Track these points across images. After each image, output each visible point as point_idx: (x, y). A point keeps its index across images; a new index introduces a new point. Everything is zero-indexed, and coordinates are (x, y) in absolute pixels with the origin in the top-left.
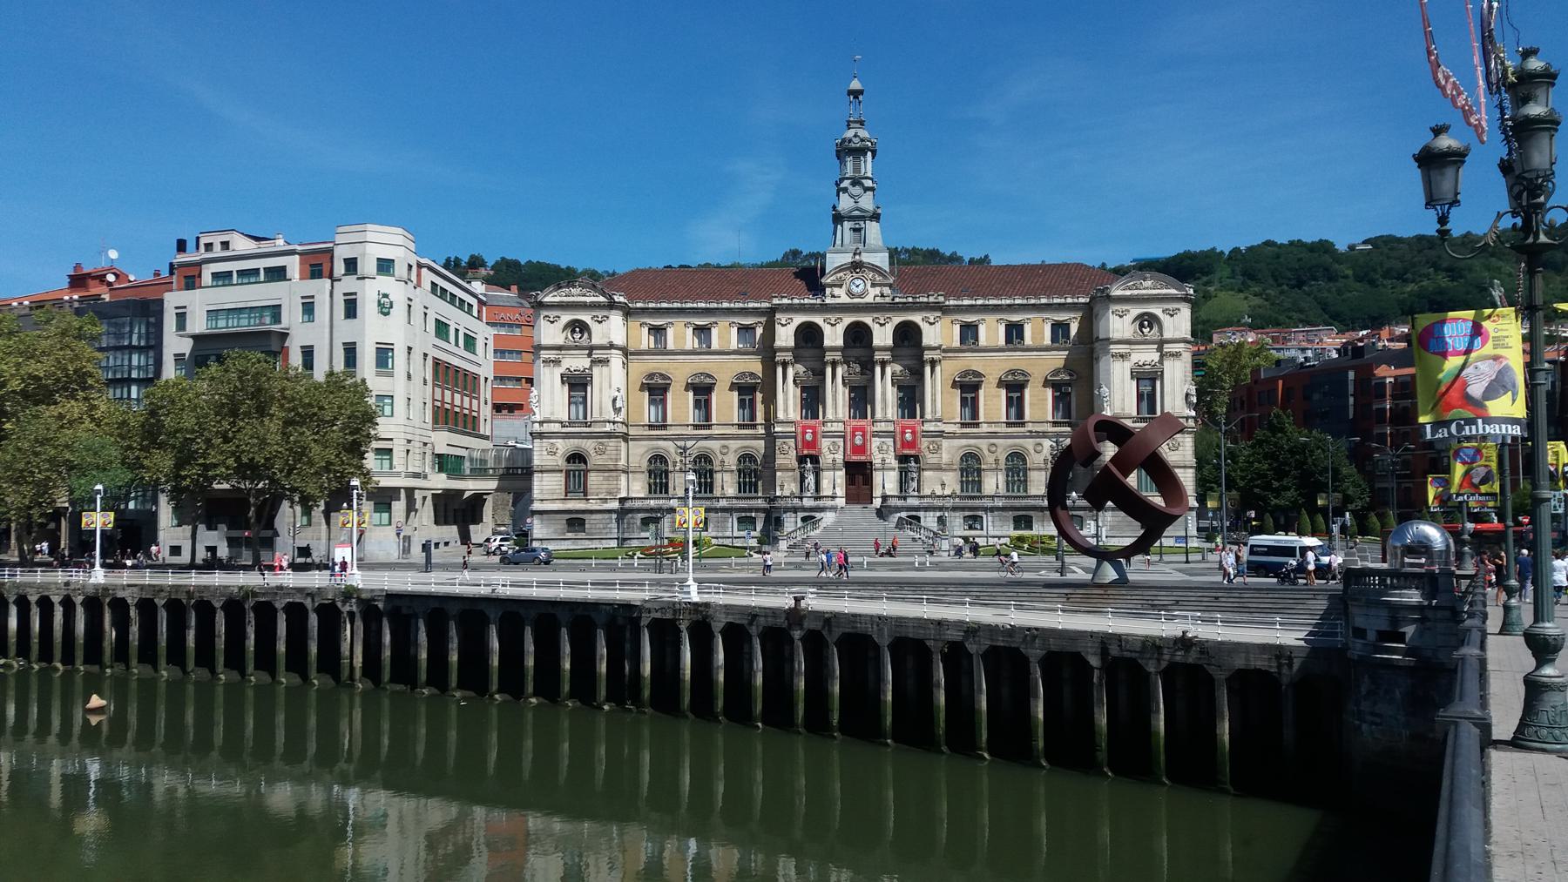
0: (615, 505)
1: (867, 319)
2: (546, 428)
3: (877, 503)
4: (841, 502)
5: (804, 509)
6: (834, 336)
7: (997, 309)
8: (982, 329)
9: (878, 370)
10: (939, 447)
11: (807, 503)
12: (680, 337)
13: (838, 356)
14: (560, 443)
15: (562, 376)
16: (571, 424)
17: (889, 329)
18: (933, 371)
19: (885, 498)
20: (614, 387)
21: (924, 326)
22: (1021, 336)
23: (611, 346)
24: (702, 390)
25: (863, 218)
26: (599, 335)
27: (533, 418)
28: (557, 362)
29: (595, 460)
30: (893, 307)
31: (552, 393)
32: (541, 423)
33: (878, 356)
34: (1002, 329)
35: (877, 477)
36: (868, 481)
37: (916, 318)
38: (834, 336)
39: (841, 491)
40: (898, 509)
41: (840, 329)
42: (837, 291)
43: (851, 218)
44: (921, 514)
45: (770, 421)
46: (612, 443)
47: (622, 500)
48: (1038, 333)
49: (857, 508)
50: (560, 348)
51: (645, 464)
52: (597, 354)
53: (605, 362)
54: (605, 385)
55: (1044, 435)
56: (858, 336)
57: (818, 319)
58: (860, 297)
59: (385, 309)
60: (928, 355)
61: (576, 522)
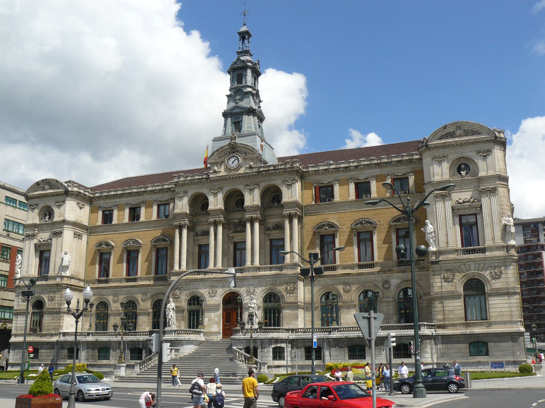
1: (241, 187)
8: (337, 189)
9: (248, 226)
22: (368, 191)
23: (64, 222)
29: (48, 304)
34: (352, 187)
41: (220, 196)
56: (235, 200)
57: (205, 191)
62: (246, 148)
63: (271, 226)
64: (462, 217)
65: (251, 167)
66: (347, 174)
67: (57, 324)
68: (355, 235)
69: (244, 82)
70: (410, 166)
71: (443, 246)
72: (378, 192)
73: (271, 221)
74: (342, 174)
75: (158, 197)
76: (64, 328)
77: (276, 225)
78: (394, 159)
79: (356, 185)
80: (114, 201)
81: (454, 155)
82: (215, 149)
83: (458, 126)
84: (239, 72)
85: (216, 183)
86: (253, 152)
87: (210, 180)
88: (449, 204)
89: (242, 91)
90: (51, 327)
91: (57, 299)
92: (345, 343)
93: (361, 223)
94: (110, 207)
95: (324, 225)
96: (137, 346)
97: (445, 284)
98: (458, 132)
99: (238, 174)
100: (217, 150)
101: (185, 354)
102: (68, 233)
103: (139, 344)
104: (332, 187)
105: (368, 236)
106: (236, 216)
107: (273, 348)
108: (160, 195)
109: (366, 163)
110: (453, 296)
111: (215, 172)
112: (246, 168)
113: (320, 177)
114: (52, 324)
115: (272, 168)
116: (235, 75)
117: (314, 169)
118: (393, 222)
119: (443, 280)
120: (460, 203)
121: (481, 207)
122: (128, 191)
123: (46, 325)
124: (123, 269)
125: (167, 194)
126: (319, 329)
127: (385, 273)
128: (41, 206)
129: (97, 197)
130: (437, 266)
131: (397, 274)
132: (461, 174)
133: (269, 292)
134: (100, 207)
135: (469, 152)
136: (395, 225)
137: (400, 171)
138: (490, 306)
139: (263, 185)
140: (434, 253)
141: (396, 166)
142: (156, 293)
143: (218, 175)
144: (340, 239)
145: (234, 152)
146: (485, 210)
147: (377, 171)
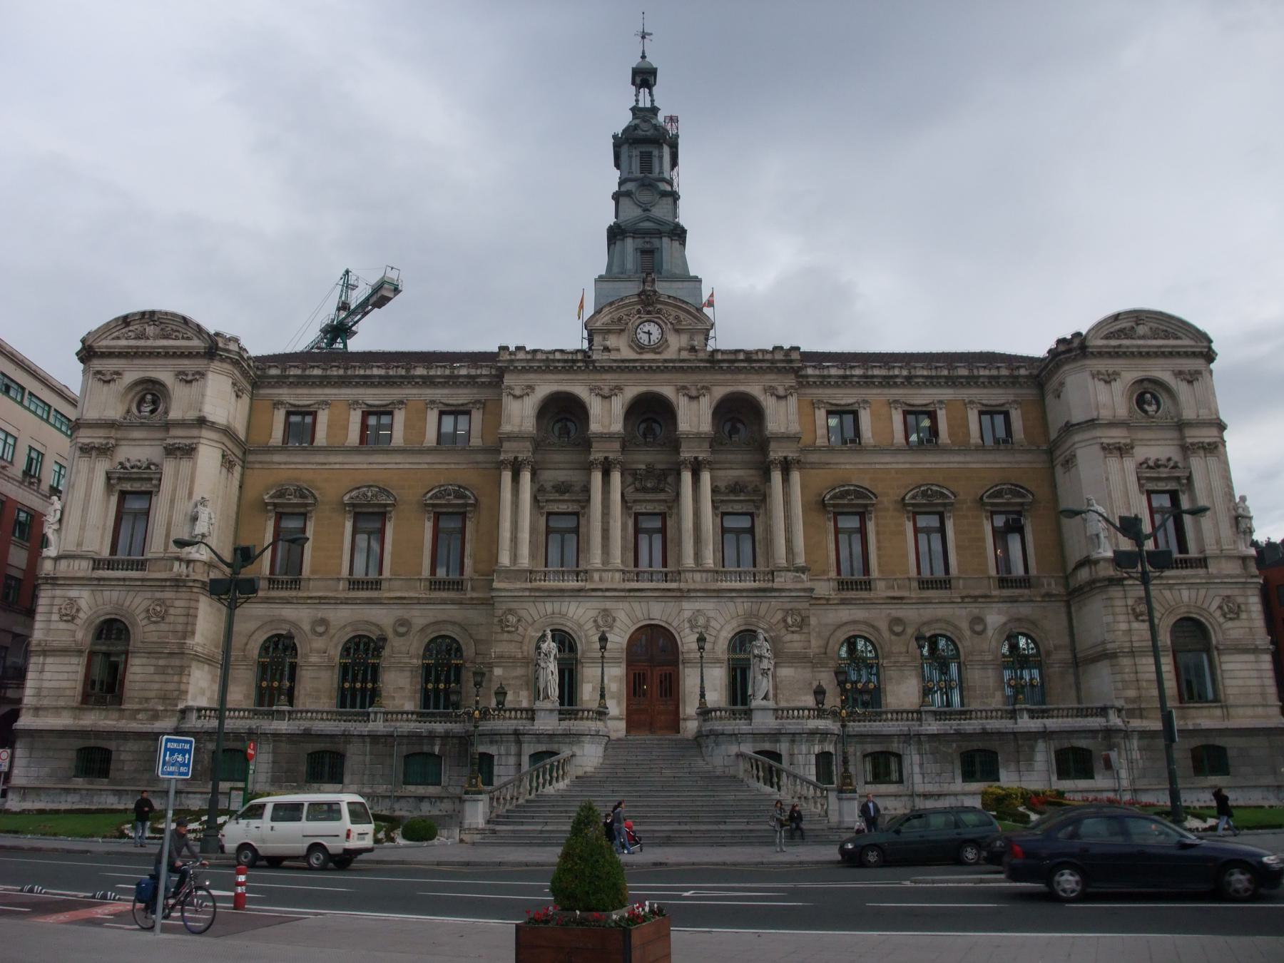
1: (668, 391)
3: (691, 727)
4: (617, 728)
5: (539, 736)
7: (888, 382)
8: (865, 417)
9: (687, 477)
10: (803, 623)
11: (547, 723)
12: (338, 426)
13: (614, 451)
14: (84, 597)
15: (109, 477)
16: (110, 565)
17: (705, 407)
18: (786, 480)
19: (705, 712)
20: (197, 497)
21: (769, 403)
25: (659, 234)
27: (46, 552)
29: (144, 632)
31: (85, 510)
32: (57, 559)
33: (686, 454)
34: (897, 417)
35: (689, 680)
36: (670, 687)
37: (754, 388)
38: (606, 416)
39: (615, 708)
40: (735, 737)
41: (618, 406)
42: (612, 341)
43: (637, 233)
44: (783, 747)
45: (490, 569)
46: (179, 602)
47: (184, 712)
48: (959, 426)
49: (644, 737)
51: (254, 649)
54: (182, 493)
56: (651, 415)
57: (581, 391)
58: (654, 350)
60: (776, 453)
62: (680, 308)
63: (722, 485)
64: (1153, 496)
65: (693, 349)
66: (886, 391)
67: (171, 687)
68: (908, 518)
69: (657, 170)
70: (1011, 391)
72: (950, 435)
73: (721, 473)
74: (875, 391)
75: (440, 394)
76: (189, 696)
77: (737, 483)
78: (982, 372)
79: (906, 413)
80: (318, 391)
82: (604, 301)
84: (645, 148)
85: (608, 376)
86: (695, 317)
87: (595, 367)
89: (656, 188)
90: (152, 694)
91: (171, 619)
92: (954, 745)
93: (924, 494)
94: (309, 406)
95: (848, 493)
96: (426, 749)
97: (1135, 625)
99: (666, 361)
100: (611, 304)
101: (588, 769)
102: (209, 456)
103: (433, 745)
104: (855, 414)
105: (934, 522)
106: (642, 459)
107: (817, 756)
108: (445, 391)
109: (925, 373)
111: (607, 349)
112: (680, 350)
113: (829, 391)
114: (156, 686)
115: (741, 356)
116: (636, 152)
117: (817, 372)
118: (989, 497)
119: (1132, 618)
120: (1149, 467)
121: (1189, 478)
122: (362, 372)
123: (137, 686)
124: (341, 557)
125: (460, 391)
126: (997, 711)
127: (975, 602)
129: (273, 377)
130: (1120, 588)
131: (1000, 605)
132: (1146, 412)
133: (743, 628)
134: (277, 404)
136: (993, 505)
137: (995, 396)
138: (1226, 675)
139: (719, 392)
141: (985, 387)
142: (433, 620)
143: (614, 356)
144: (877, 525)
145: (649, 313)
146: (1199, 483)
147: (946, 394)
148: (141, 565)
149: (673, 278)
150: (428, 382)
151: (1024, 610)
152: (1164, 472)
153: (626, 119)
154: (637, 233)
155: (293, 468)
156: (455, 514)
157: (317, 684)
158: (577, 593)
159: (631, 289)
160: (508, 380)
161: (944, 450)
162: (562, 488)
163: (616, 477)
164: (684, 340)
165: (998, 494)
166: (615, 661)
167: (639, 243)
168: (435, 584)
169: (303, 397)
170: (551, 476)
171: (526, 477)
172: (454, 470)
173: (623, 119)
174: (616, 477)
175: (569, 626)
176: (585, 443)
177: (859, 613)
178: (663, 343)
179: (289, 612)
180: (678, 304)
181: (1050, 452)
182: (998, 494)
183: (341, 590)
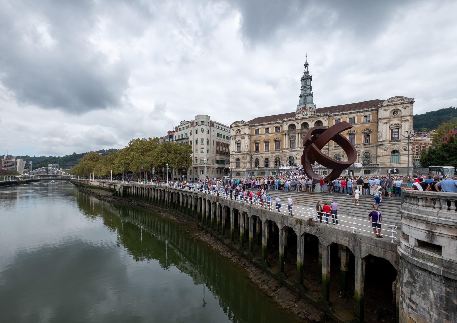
0: (245, 170)
1: (307, 122)
2: (232, 153)
6: (298, 126)
7: (346, 114)
12: (262, 131)
13: (299, 131)
21: (323, 121)
23: (245, 134)
24: (267, 143)
25: (307, 96)
26: (243, 132)
28: (235, 139)
30: (314, 117)
37: (321, 119)
38: (298, 126)
41: (300, 125)
42: (299, 115)
43: (303, 96)
46: (245, 156)
48: (359, 120)
50: (235, 136)
52: (243, 136)
53: (244, 138)
55: (361, 147)
57: (294, 123)
59: (202, 131)
61: (238, 173)
71: (384, 139)
81: (392, 108)
83: (395, 98)
88: (388, 125)
98: (395, 100)
110: (387, 155)
128: (236, 129)
135: (399, 107)
139: (316, 121)
140: (381, 141)
148: (240, 152)
149: (309, 103)
150: (273, 124)
151: (368, 149)
152: (395, 126)
153: (303, 74)
154: (303, 96)
155: (257, 137)
156: (278, 141)
157: (262, 165)
158: (294, 151)
159: (302, 106)
160: (284, 123)
161: (356, 124)
162: (293, 136)
163: (300, 135)
164: (310, 113)
165: (365, 130)
166: (299, 160)
167: (304, 98)
168: (276, 151)
169: (257, 128)
170: (291, 135)
171: (287, 136)
172: (278, 136)
173: (302, 75)
174: (300, 135)
175: (293, 155)
176: (295, 130)
177: (338, 151)
178: (307, 114)
179: (258, 155)
180: (309, 108)
181: (377, 122)
182: (365, 130)
183: (264, 152)
